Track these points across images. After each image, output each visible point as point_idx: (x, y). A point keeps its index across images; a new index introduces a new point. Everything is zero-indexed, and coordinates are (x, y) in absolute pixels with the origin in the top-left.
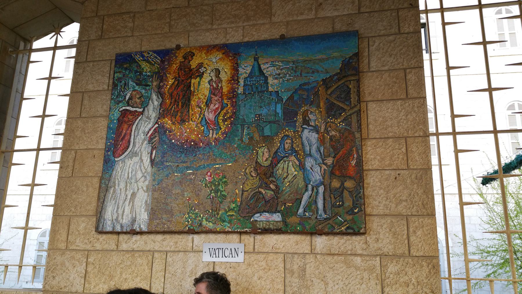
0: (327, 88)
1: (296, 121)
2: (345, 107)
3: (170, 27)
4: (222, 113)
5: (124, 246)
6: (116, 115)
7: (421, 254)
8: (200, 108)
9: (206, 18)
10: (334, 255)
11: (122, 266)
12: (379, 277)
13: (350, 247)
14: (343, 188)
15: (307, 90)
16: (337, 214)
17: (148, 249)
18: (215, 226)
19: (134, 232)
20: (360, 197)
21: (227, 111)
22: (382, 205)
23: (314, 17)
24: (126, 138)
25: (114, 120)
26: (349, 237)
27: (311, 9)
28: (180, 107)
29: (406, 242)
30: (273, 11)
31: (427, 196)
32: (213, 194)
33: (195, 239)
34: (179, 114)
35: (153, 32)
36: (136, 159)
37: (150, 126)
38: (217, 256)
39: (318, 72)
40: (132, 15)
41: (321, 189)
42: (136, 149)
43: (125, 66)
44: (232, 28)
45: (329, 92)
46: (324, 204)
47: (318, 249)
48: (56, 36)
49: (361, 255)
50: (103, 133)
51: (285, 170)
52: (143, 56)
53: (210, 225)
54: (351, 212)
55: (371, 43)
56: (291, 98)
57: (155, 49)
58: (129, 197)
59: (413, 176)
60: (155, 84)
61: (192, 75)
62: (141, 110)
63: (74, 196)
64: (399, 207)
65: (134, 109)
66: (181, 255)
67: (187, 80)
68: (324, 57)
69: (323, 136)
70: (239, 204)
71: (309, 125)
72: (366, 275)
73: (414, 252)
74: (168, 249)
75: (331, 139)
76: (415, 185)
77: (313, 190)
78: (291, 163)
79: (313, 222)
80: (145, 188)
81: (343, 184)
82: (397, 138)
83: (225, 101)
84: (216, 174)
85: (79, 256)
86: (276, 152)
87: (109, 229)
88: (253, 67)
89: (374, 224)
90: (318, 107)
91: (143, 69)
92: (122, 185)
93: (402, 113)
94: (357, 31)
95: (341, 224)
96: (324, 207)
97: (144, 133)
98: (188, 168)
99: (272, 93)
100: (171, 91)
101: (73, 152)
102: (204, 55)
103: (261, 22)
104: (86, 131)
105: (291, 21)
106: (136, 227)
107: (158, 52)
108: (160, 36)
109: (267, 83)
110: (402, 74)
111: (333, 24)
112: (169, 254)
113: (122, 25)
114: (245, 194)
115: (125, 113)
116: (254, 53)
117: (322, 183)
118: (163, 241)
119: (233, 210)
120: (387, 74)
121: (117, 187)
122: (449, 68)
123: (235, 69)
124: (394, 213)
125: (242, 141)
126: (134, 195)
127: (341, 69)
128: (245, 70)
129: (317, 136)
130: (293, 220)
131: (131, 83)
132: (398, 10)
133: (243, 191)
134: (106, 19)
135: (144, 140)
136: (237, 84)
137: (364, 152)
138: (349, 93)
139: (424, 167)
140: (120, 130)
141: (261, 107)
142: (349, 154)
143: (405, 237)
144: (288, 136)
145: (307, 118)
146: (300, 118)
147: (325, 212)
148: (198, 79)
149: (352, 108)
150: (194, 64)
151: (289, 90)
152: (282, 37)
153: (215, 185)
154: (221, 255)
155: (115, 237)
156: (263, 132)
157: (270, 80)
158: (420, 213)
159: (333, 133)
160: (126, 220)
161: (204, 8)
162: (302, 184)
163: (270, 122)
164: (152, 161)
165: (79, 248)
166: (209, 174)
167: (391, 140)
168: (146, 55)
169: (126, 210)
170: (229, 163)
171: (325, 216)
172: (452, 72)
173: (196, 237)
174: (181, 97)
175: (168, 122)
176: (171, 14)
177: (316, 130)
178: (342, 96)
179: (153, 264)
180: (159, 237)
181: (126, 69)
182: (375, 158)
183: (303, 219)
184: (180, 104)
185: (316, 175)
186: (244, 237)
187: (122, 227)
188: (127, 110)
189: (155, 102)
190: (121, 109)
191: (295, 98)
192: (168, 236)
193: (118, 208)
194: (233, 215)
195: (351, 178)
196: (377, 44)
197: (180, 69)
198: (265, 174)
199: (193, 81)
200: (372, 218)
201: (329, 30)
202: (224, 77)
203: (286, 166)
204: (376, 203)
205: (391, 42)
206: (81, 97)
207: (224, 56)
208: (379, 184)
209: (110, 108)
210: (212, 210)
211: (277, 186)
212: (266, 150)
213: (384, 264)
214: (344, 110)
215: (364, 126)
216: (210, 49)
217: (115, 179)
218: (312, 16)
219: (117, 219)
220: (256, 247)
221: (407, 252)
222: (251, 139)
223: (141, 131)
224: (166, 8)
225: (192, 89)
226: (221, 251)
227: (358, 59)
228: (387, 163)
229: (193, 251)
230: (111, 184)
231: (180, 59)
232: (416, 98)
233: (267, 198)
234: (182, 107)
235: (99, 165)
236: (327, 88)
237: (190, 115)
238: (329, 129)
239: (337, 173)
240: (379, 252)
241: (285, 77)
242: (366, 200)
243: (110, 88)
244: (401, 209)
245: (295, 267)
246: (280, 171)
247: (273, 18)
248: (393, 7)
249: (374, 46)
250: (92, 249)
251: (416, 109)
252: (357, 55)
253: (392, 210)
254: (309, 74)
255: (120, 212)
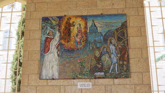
0: (117, 32)
1: (107, 42)
2: (123, 38)
3: (61, 8)
4: (82, 39)
5: (50, 84)
6: (44, 39)
7: (146, 83)
8: (74, 37)
9: (74, 6)
10: (121, 85)
11: (49, 90)
12: (134, 91)
13: (125, 82)
14: (123, 64)
15: (111, 32)
16: (121, 72)
17: (58, 85)
18: (82, 77)
19: (53, 79)
20: (129, 67)
21: (84, 38)
22: (135, 69)
23: (111, 8)
24: (48, 47)
25: (43, 40)
26: (125, 79)
27: (110, 5)
28: (67, 36)
29: (142, 80)
30: (98, 5)
31: (148, 67)
32: (81, 66)
33: (75, 82)
34: (67, 39)
35: (55, 10)
36: (52, 54)
37: (57, 43)
38: (83, 86)
39: (114, 26)
40: (47, 3)
41: (117, 64)
42: (52, 51)
43: (46, 22)
44: (83, 10)
45: (118, 33)
46: (118, 69)
47: (116, 84)
48: (12, 7)
49: (129, 85)
50: (39, 45)
51: (105, 58)
52: (52, 18)
53: (80, 77)
54: (126, 71)
55: (130, 18)
56: (105, 35)
57: (56, 16)
58: (51, 67)
59: (144, 60)
60: (57, 28)
61: (71, 25)
62: (53, 37)
63: (30, 67)
64: (140, 69)
65: (51, 37)
66: (70, 86)
67: (69, 27)
68: (116, 21)
69: (117, 47)
70: (90, 70)
71: (112, 44)
72: (130, 90)
73: (144, 83)
74: (65, 85)
75: (119, 48)
76: (144, 63)
77: (114, 65)
78: (106, 56)
79: (114, 75)
80: (56, 64)
81: (123, 63)
82: (139, 48)
83: (83, 35)
84: (81, 60)
85: (33, 87)
86: (101, 53)
87: (44, 78)
88: (92, 24)
89: (133, 75)
90: (115, 38)
91: (53, 23)
92: (48, 63)
93: (140, 41)
94: (126, 14)
95: (123, 75)
96: (118, 70)
97: (55, 45)
98: (71, 57)
99: (99, 33)
100: (63, 31)
101: (28, 52)
102: (75, 19)
103: (93, 8)
104: (32, 44)
105: (104, 9)
106: (54, 77)
107: (58, 17)
108: (58, 11)
109: (97, 29)
110: (140, 28)
111: (118, 10)
112: (66, 86)
113: (43, 6)
114: (92, 66)
115: (47, 38)
116: (92, 19)
117: (117, 63)
118: (63, 82)
119: (88, 71)
120: (135, 28)
121: (46, 64)
122: (152, 26)
123: (86, 24)
124: (138, 72)
125: (90, 48)
126: (52, 67)
127: (121, 26)
128: (90, 24)
129: (114, 47)
130: (108, 74)
131: (48, 28)
132: (138, 8)
133: (91, 65)
134: (37, 4)
135: (55, 48)
136: (87, 29)
137: (129, 53)
138: (124, 34)
139: (146, 57)
140: (46, 44)
141: (95, 37)
142: (125, 53)
143: (142, 78)
144: (105, 47)
145: (111, 42)
146: (109, 41)
147: (118, 71)
148: (73, 27)
149: (125, 39)
150: (71, 22)
151: (105, 32)
152: (102, 14)
153: (81, 63)
154: (84, 86)
155: (46, 81)
156: (97, 46)
157: (98, 28)
158: (146, 71)
159: (120, 47)
160: (50, 75)
161: (73, 2)
162: (110, 63)
163: (99, 42)
164: (58, 55)
165: (33, 85)
166: (79, 59)
167: (137, 49)
168: (53, 18)
169: (50, 72)
170: (86, 56)
171: (118, 73)
172: (153, 27)
173: (75, 80)
174: (67, 33)
175: (63, 42)
176: (61, 4)
177: (114, 45)
178: (122, 35)
179: (61, 90)
180: (62, 81)
181: (46, 23)
182: (132, 55)
183: (111, 74)
184: (67, 35)
185: (115, 60)
186: (91, 80)
187: (49, 77)
188: (48, 37)
189: (58, 34)
190: (45, 37)
191: (107, 35)
192: (65, 80)
193: (47, 71)
194: (88, 73)
195: (125, 61)
196: (132, 18)
197: (66, 23)
198: (98, 60)
199: (71, 28)
200: (132, 73)
201: (116, 13)
202: (83, 26)
203: (105, 57)
204: (133, 68)
205: (136, 18)
206: (29, 32)
207: (82, 19)
208: (134, 63)
209: (41, 36)
210: (81, 71)
211: (102, 64)
212: (98, 52)
213: (135, 87)
214: (123, 39)
215: (129, 44)
216: (77, 17)
217: (45, 61)
218: (111, 7)
219: (47, 75)
220: (96, 83)
221: (142, 83)
222: (93, 48)
223: (53, 45)
224: (60, 2)
225: (71, 30)
226: (84, 85)
227: (126, 23)
228: (136, 56)
229: (74, 85)
230: (44, 63)
231: (66, 20)
232: (144, 36)
233: (99, 68)
234: (68, 37)
235: (38, 56)
236: (117, 32)
237: (71, 39)
238: (118, 45)
239: (121, 59)
240: (134, 83)
241: (103, 27)
242: (130, 68)
243: (41, 29)
244: (141, 70)
245: (109, 89)
246: (103, 59)
247: (98, 7)
248: (136, 7)
249: (131, 19)
250: (38, 85)
251: (144, 40)
252: (126, 21)
253: (138, 70)
254: (111, 27)
255: (48, 72)
